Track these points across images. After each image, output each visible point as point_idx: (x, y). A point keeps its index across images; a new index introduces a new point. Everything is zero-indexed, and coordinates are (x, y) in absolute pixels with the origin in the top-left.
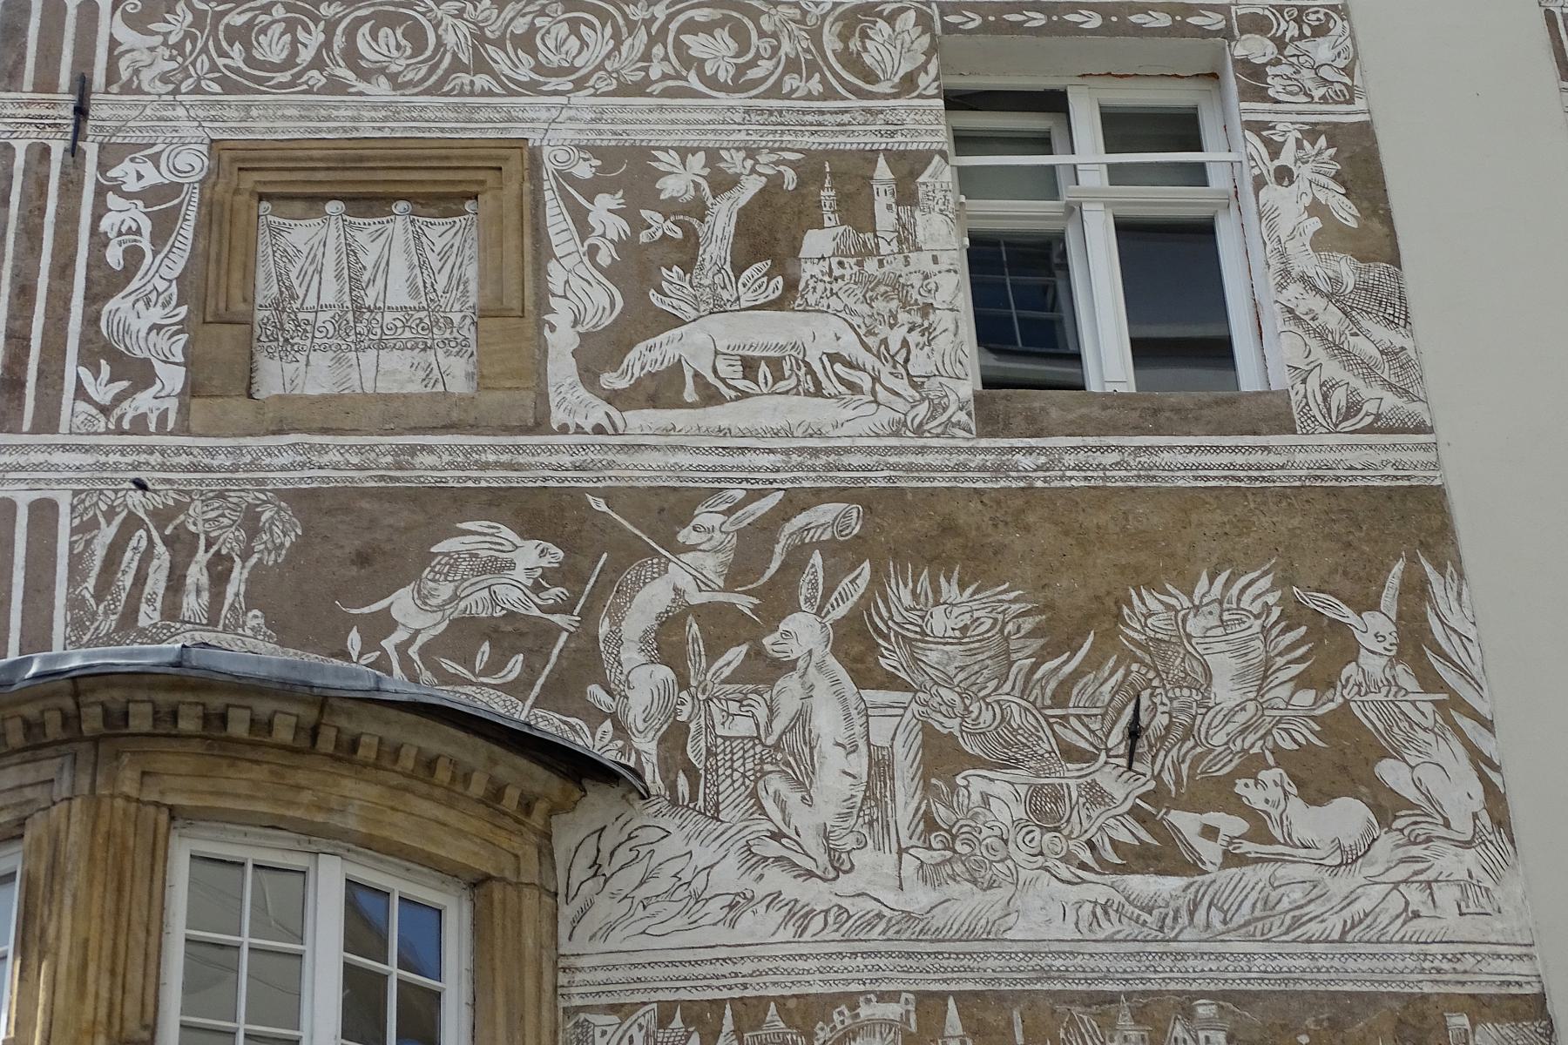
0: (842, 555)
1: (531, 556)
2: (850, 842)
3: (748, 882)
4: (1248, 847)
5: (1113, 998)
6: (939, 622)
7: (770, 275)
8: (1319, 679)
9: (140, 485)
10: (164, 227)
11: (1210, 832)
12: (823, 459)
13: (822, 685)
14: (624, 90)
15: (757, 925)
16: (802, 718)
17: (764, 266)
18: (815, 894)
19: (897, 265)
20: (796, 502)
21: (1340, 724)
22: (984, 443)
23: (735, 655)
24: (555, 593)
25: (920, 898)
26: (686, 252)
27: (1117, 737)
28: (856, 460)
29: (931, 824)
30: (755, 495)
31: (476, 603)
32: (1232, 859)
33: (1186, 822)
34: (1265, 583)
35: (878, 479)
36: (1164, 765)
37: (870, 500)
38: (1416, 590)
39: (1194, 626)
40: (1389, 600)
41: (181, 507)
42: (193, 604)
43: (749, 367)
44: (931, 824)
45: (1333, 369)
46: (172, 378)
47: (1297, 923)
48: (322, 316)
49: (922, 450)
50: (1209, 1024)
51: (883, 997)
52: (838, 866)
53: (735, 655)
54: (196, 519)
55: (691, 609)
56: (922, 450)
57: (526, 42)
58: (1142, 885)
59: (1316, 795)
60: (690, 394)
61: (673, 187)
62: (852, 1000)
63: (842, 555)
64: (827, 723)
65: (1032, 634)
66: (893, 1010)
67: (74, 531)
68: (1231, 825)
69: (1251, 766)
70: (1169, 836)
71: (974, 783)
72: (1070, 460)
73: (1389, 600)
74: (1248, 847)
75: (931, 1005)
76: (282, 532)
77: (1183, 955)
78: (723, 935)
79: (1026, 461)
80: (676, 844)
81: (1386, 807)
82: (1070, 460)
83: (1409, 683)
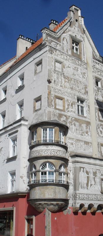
0: (74, 120)
1: (65, 118)
6: (77, 124)
10: (53, 98)
14: (68, 96)
18: (73, 134)
20: (73, 117)
21: (87, 131)
26: (69, 105)
37: (75, 118)
38: (89, 126)
42: (55, 117)
43: (71, 111)
45: (88, 116)
46: (54, 106)
54: (55, 113)
57: (64, 93)
58: (82, 136)
61: (69, 102)
63: (74, 120)
76: (58, 115)
81: (88, 135)
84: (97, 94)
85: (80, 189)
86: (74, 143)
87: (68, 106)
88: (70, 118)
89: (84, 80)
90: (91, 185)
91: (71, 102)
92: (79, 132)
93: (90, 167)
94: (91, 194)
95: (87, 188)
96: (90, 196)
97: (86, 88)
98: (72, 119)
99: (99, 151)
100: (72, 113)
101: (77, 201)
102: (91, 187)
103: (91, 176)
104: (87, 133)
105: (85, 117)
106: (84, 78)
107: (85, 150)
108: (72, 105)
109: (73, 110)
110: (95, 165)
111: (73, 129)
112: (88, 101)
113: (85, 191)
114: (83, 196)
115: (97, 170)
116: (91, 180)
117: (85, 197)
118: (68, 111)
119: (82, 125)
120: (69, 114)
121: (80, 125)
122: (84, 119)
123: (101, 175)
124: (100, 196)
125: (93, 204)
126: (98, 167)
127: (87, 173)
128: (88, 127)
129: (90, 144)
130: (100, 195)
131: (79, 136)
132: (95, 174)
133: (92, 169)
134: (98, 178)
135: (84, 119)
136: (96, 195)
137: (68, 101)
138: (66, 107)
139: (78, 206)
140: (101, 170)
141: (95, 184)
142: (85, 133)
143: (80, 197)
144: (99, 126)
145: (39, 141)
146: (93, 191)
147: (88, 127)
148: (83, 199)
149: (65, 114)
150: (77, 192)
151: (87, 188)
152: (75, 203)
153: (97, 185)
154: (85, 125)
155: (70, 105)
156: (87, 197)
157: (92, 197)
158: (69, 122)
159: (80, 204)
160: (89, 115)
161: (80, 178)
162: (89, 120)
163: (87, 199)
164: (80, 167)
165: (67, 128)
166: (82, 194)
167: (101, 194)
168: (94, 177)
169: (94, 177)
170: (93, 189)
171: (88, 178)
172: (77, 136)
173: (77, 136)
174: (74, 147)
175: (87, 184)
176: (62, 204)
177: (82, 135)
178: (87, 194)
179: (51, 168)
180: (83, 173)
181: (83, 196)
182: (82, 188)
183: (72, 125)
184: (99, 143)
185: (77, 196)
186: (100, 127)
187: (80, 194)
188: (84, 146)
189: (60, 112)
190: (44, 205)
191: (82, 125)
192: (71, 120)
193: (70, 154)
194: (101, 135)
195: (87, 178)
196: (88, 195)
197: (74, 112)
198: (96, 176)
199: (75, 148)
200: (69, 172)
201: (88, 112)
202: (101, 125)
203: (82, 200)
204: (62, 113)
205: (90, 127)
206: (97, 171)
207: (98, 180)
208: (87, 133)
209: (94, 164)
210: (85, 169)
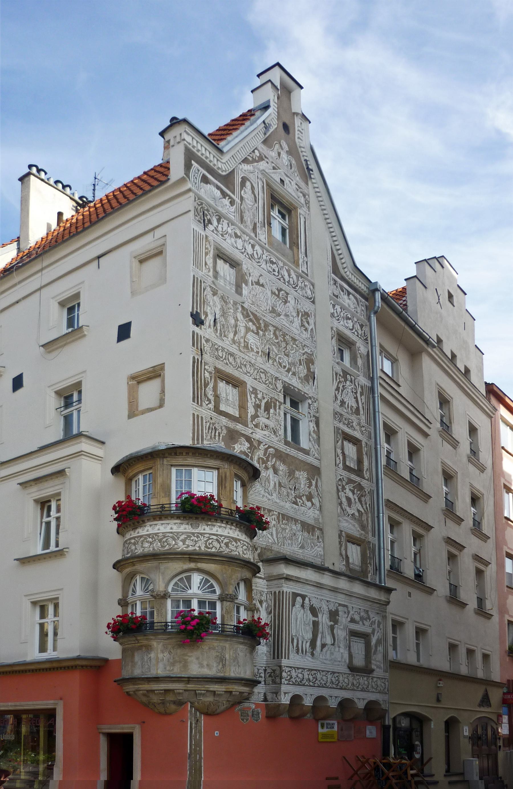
0: (274, 456)
1: (247, 445)
2: (273, 492)
3: (264, 494)
4: (302, 505)
5: (293, 518)
6: (281, 468)
7: (267, 414)
8: (309, 487)
9: (211, 418)
11: (300, 502)
12: (272, 442)
13: (271, 472)
15: (265, 499)
16: (269, 475)
17: (267, 412)
18: (269, 497)
19: (278, 418)
20: (270, 447)
21: (310, 493)
22: (285, 446)
23: (264, 465)
24: (249, 450)
25: (278, 501)
27: (293, 488)
28: (274, 444)
29: (279, 493)
30: (266, 445)
31: (242, 449)
32: (301, 506)
33: (298, 500)
34: (306, 474)
35: (276, 447)
36: (297, 492)
37: (276, 450)
39: (301, 477)
40: (315, 480)
41: (215, 423)
43: (266, 426)
44: (279, 493)
47: (306, 515)
48: (224, 399)
49: (280, 445)
50: (299, 523)
51: (276, 512)
52: (272, 495)
53: (264, 465)
55: (261, 458)
56: (280, 445)
58: (294, 505)
59: (308, 501)
60: (261, 428)
62: (273, 511)
63: (274, 456)
64: (271, 477)
65: (288, 473)
66: (276, 513)
67: (205, 422)
68: (301, 502)
69: (303, 495)
70: (296, 500)
71: (283, 489)
72: (292, 451)
73: (315, 480)
74: (302, 505)
75: (279, 513)
77: (297, 515)
78: (262, 499)
79: (288, 450)
80: (258, 487)
81: (313, 504)
82: (292, 451)
83: (316, 490)
84: (341, 387)
85: (291, 656)
86: (274, 522)
87: (256, 411)
88: (262, 447)
89: (304, 336)
90: (323, 646)
91: (264, 398)
92: (288, 493)
93: (322, 596)
94: (323, 671)
95: (313, 654)
96: (319, 676)
97: (310, 361)
98: (266, 450)
99: (341, 554)
100: (266, 433)
101: (284, 688)
102: (322, 650)
103: (324, 619)
104: (310, 498)
105: (306, 452)
106: (306, 330)
107: (302, 547)
108: (267, 409)
109: (271, 424)
110: (334, 590)
111: (269, 483)
112: (315, 404)
113: (307, 662)
114: (300, 676)
115: (340, 605)
116: (322, 633)
117: (306, 676)
118: (256, 426)
119: (297, 472)
120: (259, 435)
121: (291, 474)
122: (301, 456)
123: (349, 619)
124: (346, 676)
125: (327, 697)
126: (341, 599)
127: (314, 611)
128: (314, 483)
129: (317, 533)
130: (345, 674)
131: (288, 505)
132: (334, 615)
133: (328, 601)
134: (342, 627)
135: (301, 456)
136: (336, 675)
137: (256, 394)
138: (251, 411)
139: (285, 700)
140: (350, 606)
141: (333, 644)
142: (304, 498)
143: (291, 677)
144: (344, 483)
145: (163, 507)
146: (328, 662)
147: (314, 483)
148: (301, 681)
149: (248, 431)
150: (284, 662)
151: (313, 654)
152: (277, 693)
153: (339, 647)
154: (305, 475)
155: (263, 407)
156: (311, 678)
157: (324, 678)
158: (259, 459)
159: (291, 695)
160: (316, 447)
161: (293, 625)
162: (316, 463)
163: (311, 684)
164: (293, 593)
165: (255, 474)
166: (298, 668)
167: (348, 671)
168: (332, 623)
169: (332, 623)
170: (328, 656)
171: (315, 624)
172: (282, 504)
173: (282, 504)
174: (272, 535)
175: (313, 643)
176: (241, 693)
177: (295, 503)
178: (312, 670)
179: (203, 590)
180: (302, 610)
181: (300, 676)
182: (298, 652)
183: (267, 468)
184: (341, 531)
185: (284, 674)
186: (347, 487)
187: (291, 667)
188: (300, 536)
189: (232, 425)
190: (182, 693)
191: (297, 472)
192: (265, 454)
193: (259, 555)
194: (348, 508)
195: (311, 626)
196: (313, 672)
197: (274, 432)
198: (336, 622)
199: (276, 539)
200: (258, 605)
201: (315, 436)
202: (350, 481)
203: (299, 685)
204: (239, 427)
205: (319, 484)
206: (340, 608)
207: (341, 633)
208: (310, 498)
209: (332, 587)
210: (307, 599)
